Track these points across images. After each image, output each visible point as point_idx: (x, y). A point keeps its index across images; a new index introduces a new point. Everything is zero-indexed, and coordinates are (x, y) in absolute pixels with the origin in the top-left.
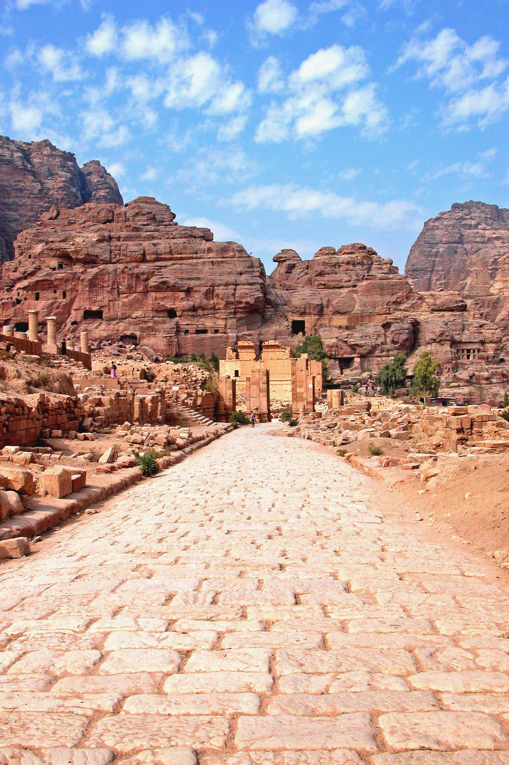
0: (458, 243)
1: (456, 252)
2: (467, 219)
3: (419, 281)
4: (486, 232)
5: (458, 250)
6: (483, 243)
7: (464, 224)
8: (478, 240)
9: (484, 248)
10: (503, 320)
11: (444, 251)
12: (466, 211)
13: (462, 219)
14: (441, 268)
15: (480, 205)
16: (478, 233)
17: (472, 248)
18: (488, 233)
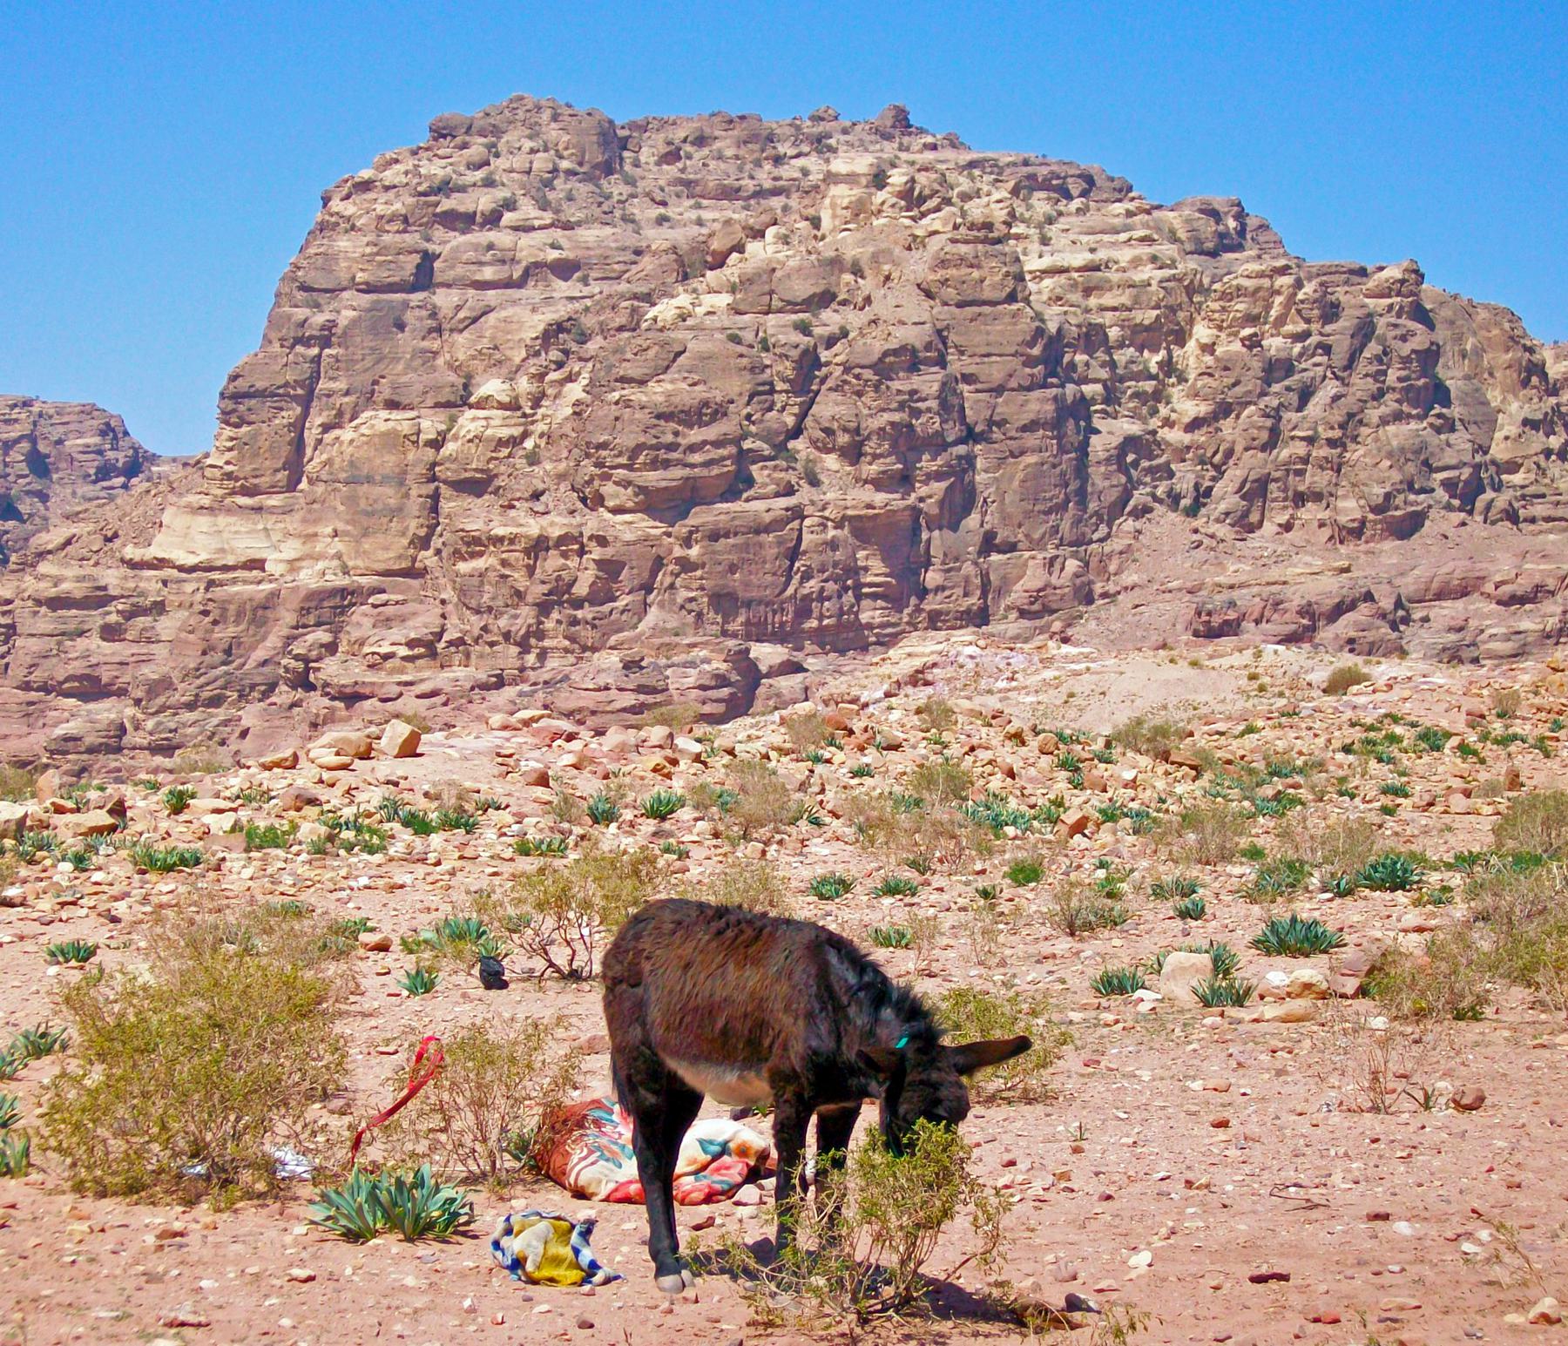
0: (413, 288)
1: (401, 326)
2: (462, 189)
3: (255, 436)
4: (525, 240)
5: (409, 317)
6: (508, 284)
7: (445, 213)
8: (488, 273)
9: (502, 306)
10: (264, 663)
11: (354, 322)
12: (477, 149)
13: (446, 187)
14: (341, 385)
15: (546, 115)
16: (490, 247)
17: (459, 308)
18: (531, 247)
